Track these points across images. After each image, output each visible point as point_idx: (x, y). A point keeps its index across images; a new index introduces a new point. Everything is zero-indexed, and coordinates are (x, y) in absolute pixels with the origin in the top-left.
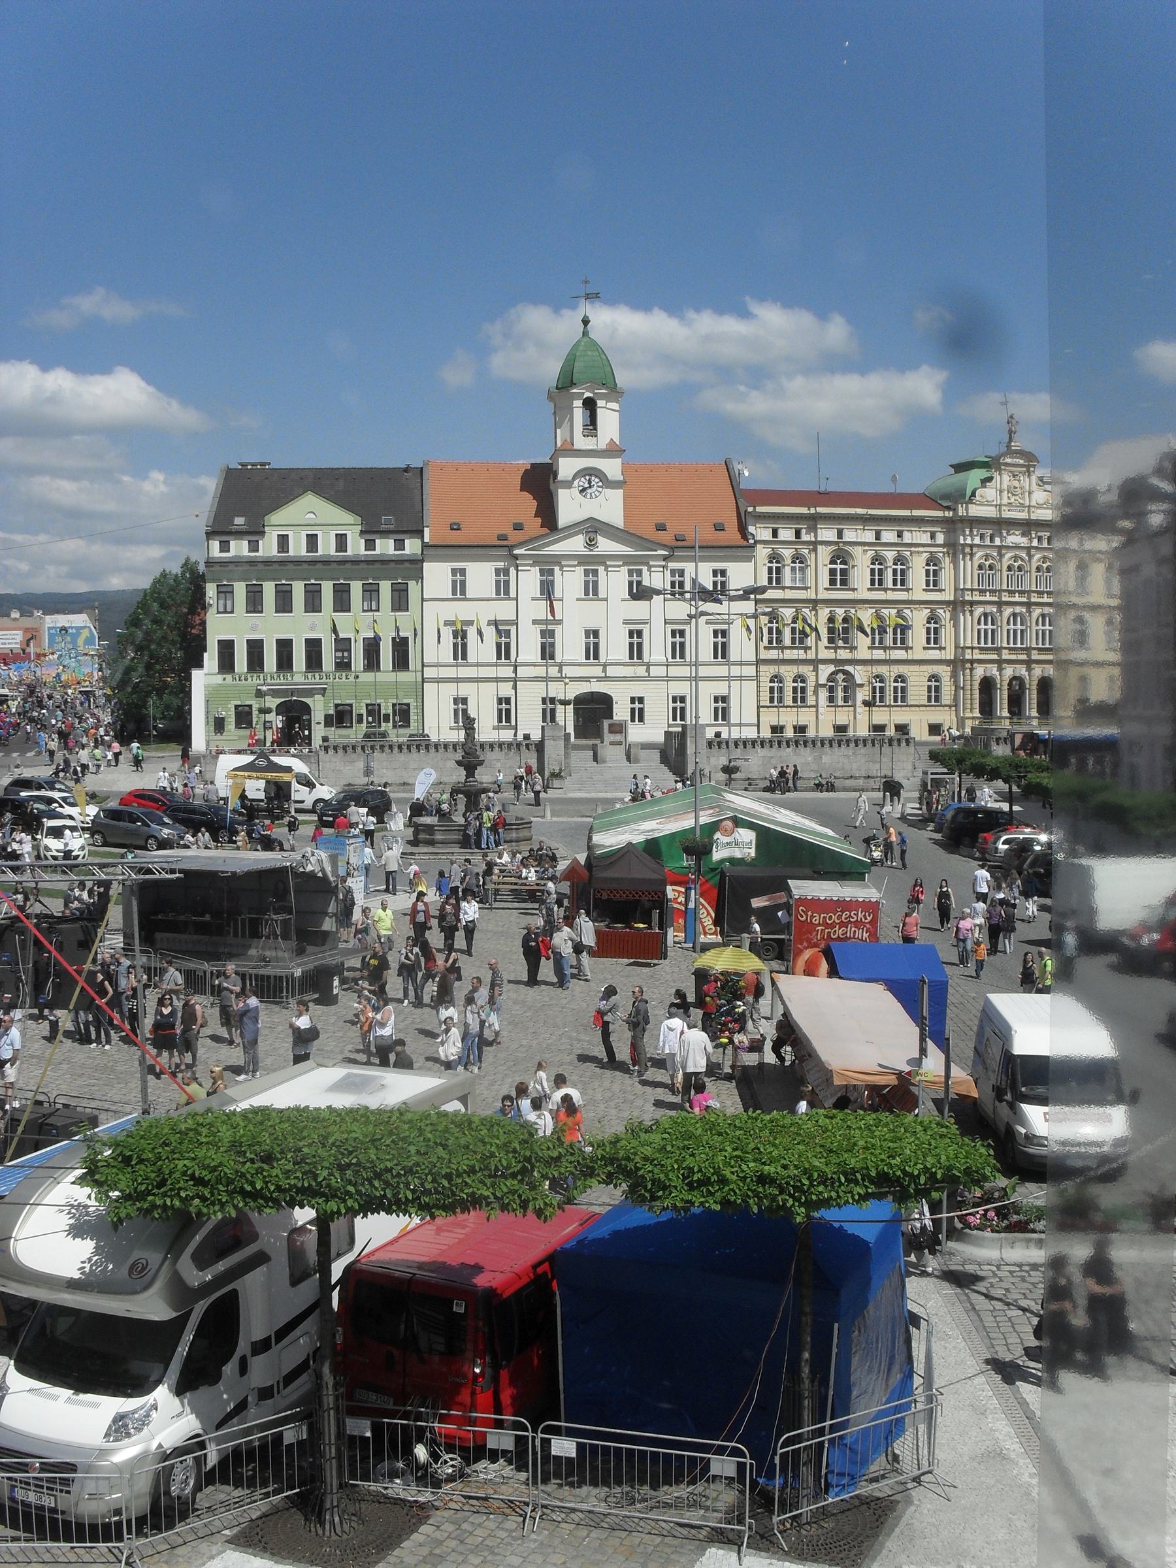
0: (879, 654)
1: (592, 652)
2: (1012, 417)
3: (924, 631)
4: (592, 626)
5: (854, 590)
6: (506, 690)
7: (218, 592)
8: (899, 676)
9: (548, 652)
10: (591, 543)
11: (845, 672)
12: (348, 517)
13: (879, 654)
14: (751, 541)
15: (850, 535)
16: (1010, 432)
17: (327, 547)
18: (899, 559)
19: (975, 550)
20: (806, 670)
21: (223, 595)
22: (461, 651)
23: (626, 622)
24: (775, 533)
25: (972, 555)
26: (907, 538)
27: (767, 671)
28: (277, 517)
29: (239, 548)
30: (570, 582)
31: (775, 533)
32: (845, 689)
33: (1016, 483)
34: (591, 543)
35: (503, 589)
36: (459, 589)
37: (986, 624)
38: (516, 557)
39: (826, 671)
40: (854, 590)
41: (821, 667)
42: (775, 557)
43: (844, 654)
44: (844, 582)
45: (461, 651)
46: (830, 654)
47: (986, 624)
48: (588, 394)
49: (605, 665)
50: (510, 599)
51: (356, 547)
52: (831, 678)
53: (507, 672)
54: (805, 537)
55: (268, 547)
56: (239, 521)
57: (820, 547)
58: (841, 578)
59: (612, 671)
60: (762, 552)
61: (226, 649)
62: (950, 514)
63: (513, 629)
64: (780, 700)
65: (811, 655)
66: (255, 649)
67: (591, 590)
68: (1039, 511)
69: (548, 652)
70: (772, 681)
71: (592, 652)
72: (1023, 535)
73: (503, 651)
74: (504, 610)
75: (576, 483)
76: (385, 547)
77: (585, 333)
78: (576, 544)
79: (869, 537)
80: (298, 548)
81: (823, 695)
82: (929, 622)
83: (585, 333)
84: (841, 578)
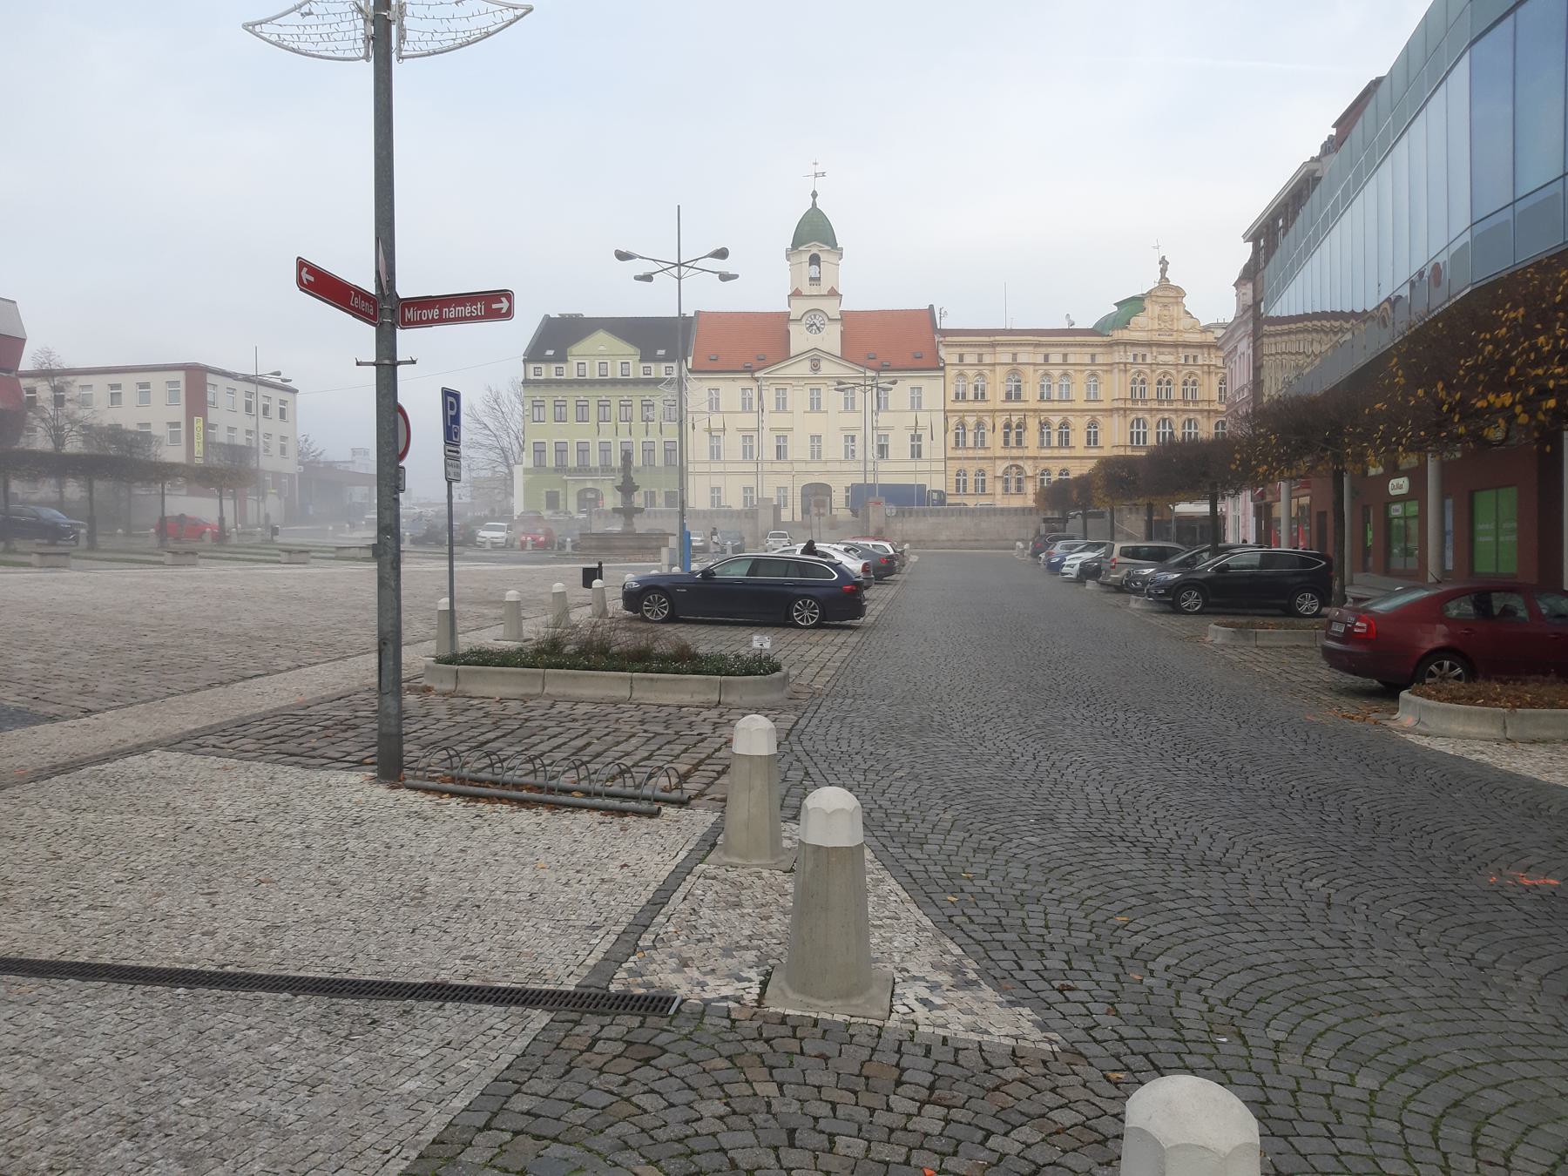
0: (1047, 452)
1: (816, 454)
2: (1163, 257)
3: (1085, 434)
4: (814, 433)
5: (1025, 401)
6: (750, 481)
7: (534, 406)
8: (1064, 470)
9: (780, 452)
10: (815, 367)
11: (1018, 467)
12: (629, 349)
13: (1047, 452)
14: (942, 365)
15: (1022, 358)
16: (1163, 271)
17: (615, 372)
18: (1065, 374)
19: (1129, 366)
20: (984, 465)
21: (536, 410)
22: (715, 454)
23: (842, 429)
24: (961, 357)
25: (1126, 371)
26: (1071, 359)
27: (954, 466)
28: (577, 349)
29: (548, 371)
30: (799, 398)
31: (961, 357)
32: (1019, 481)
33: (1166, 312)
34: (815, 367)
35: (746, 407)
36: (714, 406)
37: (1138, 427)
38: (757, 380)
39: (1001, 467)
40: (1025, 401)
41: (998, 462)
42: (961, 374)
43: (1015, 453)
44: (1018, 397)
45: (715, 454)
46: (1006, 453)
47: (1138, 427)
48: (815, 251)
49: (826, 462)
50: (752, 412)
51: (636, 370)
52: (1005, 472)
53: (752, 467)
54: (987, 359)
55: (570, 371)
56: (550, 353)
57: (998, 368)
58: (1014, 395)
59: (830, 467)
60: (951, 372)
61: (539, 450)
62: (1109, 339)
63: (755, 434)
64: (965, 490)
65: (989, 454)
66: (561, 450)
67: (815, 406)
68: (1186, 335)
69: (780, 452)
70: (958, 475)
71: (816, 454)
72: (1170, 354)
73: (748, 452)
74: (749, 421)
75: (804, 320)
76: (658, 370)
77: (814, 204)
78: (803, 368)
79: (1040, 359)
80: (592, 373)
81: (999, 486)
82: (1090, 427)
83: (814, 204)
84: (1014, 395)
